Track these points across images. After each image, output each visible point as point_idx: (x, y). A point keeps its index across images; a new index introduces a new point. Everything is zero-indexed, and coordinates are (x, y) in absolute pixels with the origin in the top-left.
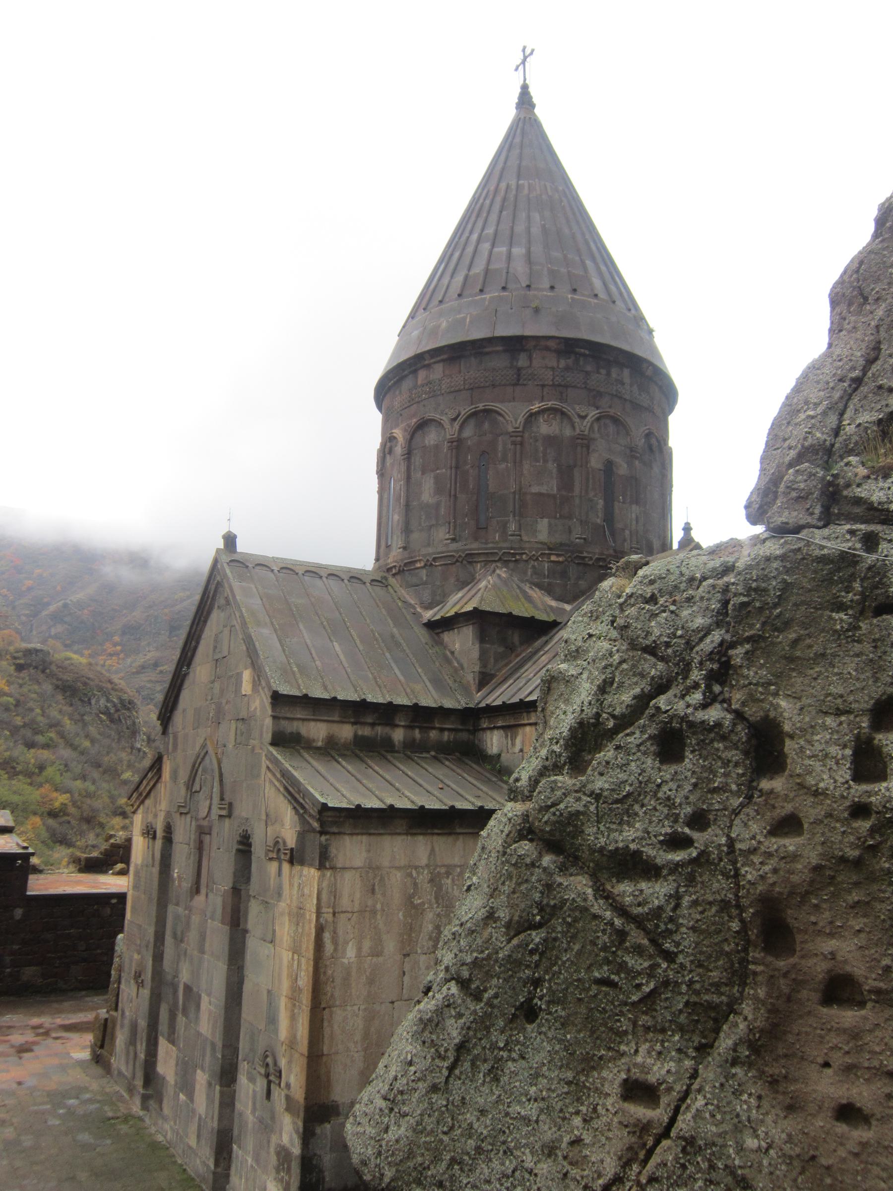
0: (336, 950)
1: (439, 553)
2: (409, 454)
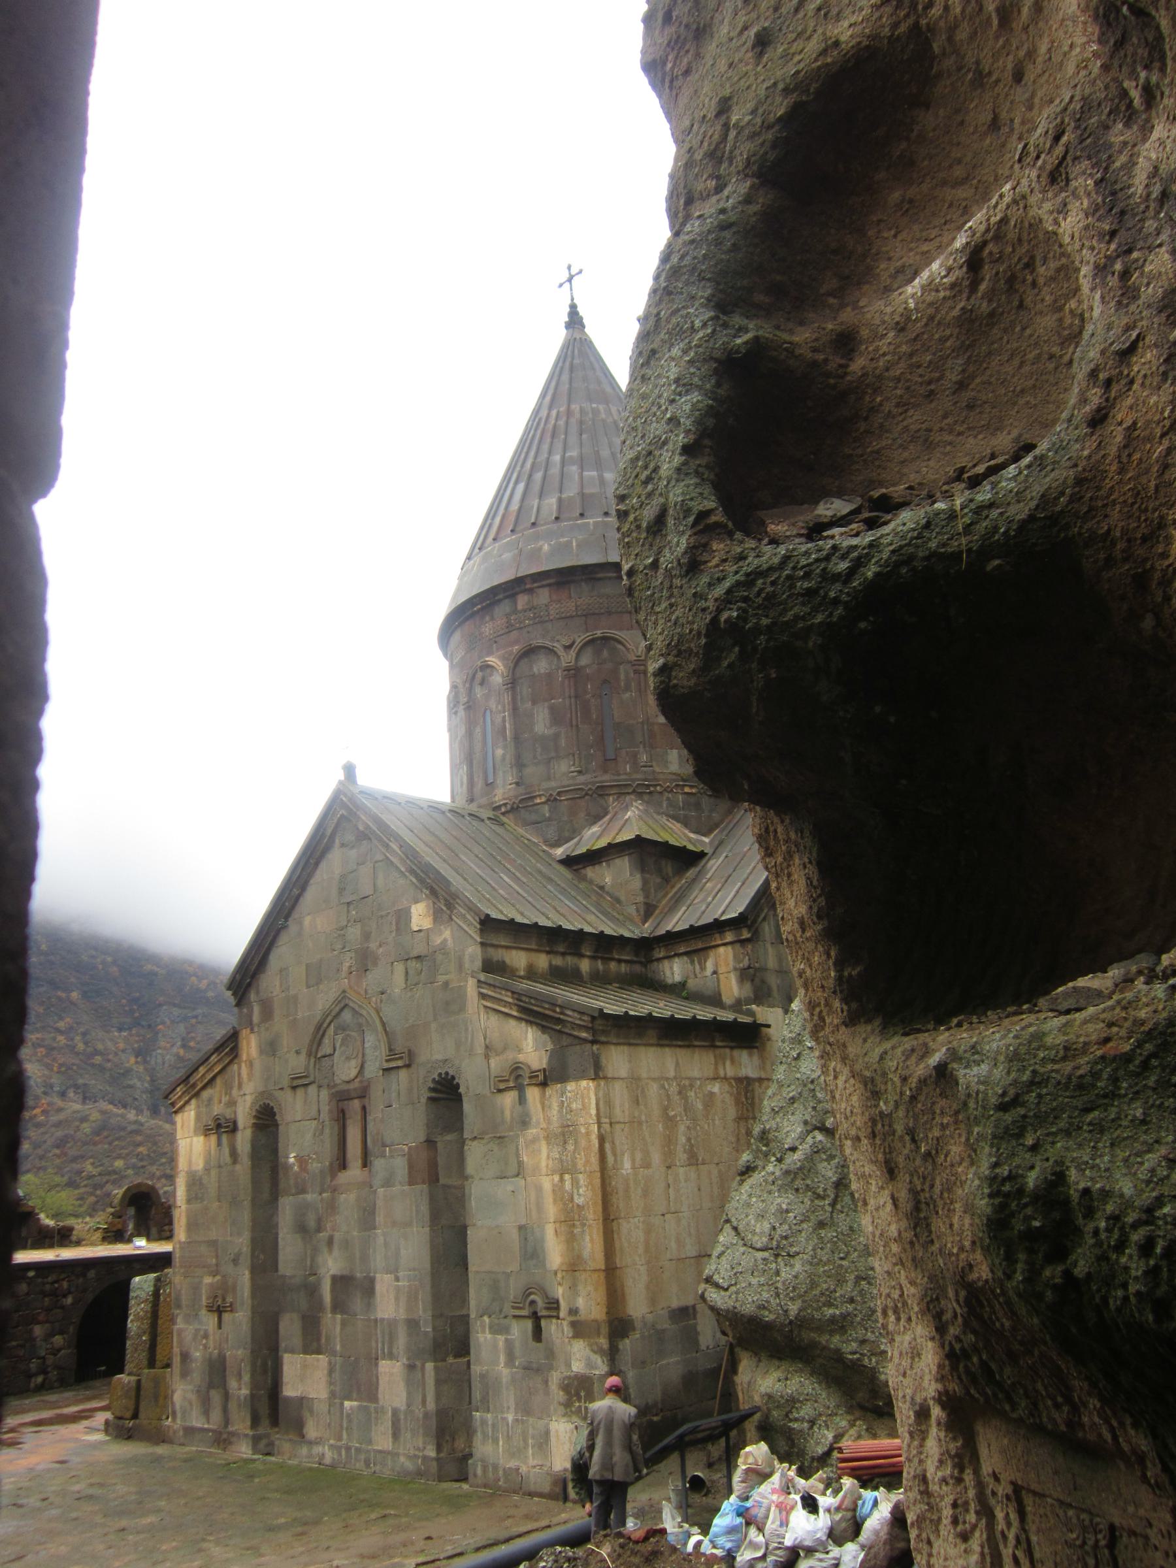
0: (616, 1160)
2: (512, 683)
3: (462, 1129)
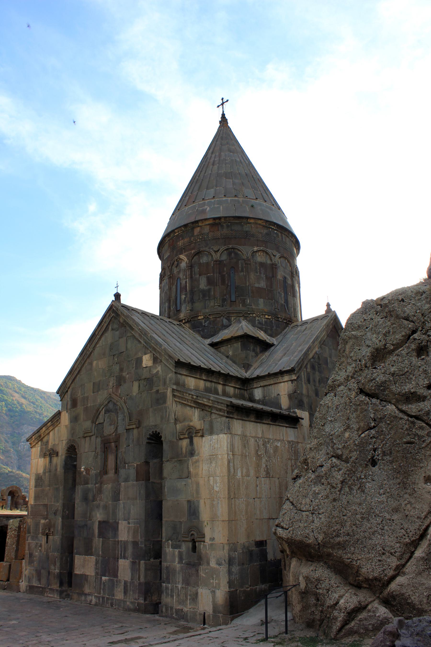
0: (234, 472)
1: (212, 312)
2: (191, 266)
3: (162, 457)
